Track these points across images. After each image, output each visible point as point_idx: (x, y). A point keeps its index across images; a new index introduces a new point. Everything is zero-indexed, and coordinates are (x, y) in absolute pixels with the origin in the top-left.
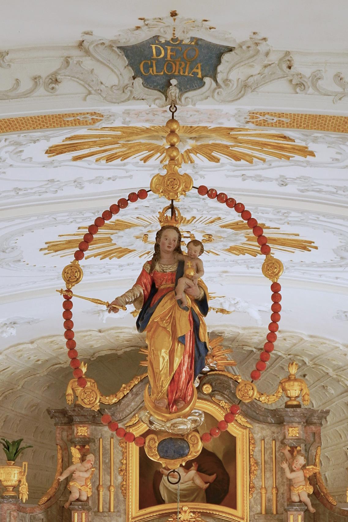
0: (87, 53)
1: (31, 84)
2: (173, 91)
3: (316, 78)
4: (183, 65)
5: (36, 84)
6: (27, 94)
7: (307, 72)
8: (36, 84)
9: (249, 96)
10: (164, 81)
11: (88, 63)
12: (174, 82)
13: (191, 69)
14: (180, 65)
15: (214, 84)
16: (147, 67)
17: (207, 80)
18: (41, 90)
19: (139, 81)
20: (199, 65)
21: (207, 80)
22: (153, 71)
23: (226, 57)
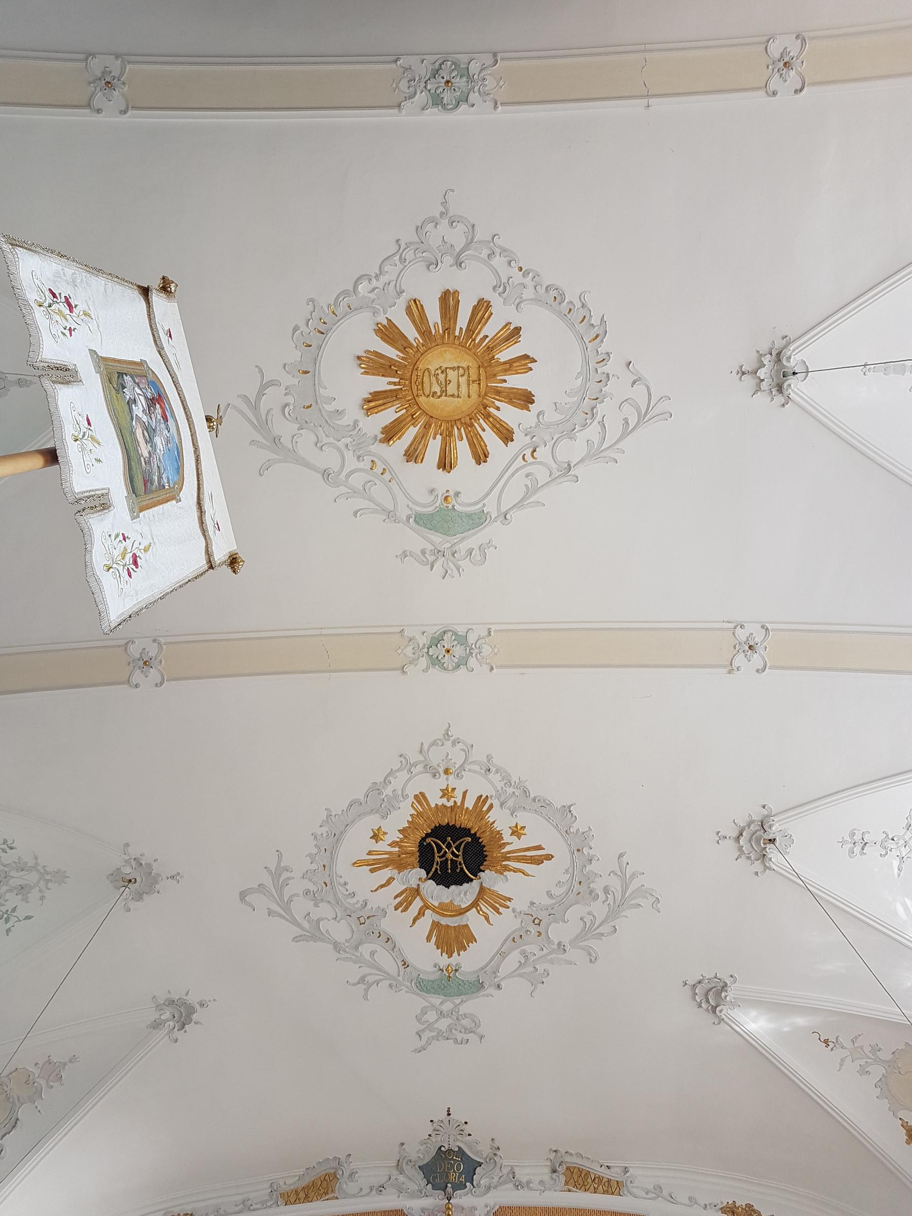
0: (401, 1172)
1: (368, 1190)
2: (449, 1189)
3: (528, 1183)
4: (454, 1176)
5: (371, 1190)
6: (367, 1195)
7: (524, 1180)
8: (371, 1190)
9: (492, 1193)
10: (443, 1186)
11: (401, 1178)
12: (449, 1185)
13: (459, 1179)
14: (453, 1175)
15: (472, 1187)
16: (434, 1178)
17: (468, 1184)
18: (374, 1192)
19: (430, 1186)
20: (463, 1176)
21: (468, 1184)
22: (438, 1181)
23: (478, 1170)
